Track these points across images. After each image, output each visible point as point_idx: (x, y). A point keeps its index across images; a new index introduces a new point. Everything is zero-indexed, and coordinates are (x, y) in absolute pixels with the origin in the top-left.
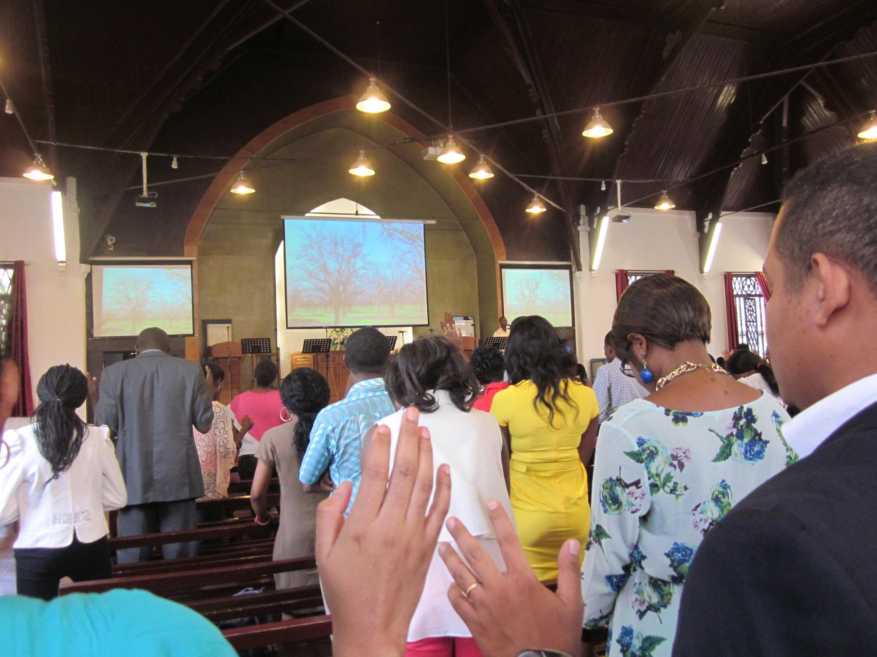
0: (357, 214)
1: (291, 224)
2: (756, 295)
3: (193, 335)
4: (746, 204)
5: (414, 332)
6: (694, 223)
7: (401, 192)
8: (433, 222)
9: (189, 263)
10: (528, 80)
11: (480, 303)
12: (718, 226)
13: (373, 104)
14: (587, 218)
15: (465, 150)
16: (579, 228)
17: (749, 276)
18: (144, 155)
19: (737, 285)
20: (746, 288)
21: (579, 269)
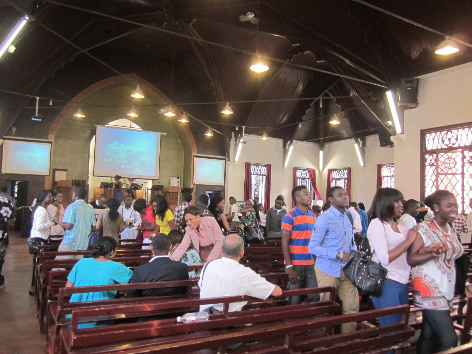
0: (130, 127)
1: (99, 128)
2: (307, 178)
3: (49, 176)
4: (307, 138)
5: (152, 182)
6: (282, 144)
7: (150, 122)
8: (165, 134)
9: (50, 142)
10: (211, 79)
12: (292, 147)
13: (138, 96)
14: (234, 138)
15: (175, 112)
16: (231, 142)
17: (304, 170)
18: (38, 98)
19: (299, 174)
20: (303, 175)
21: (229, 161)
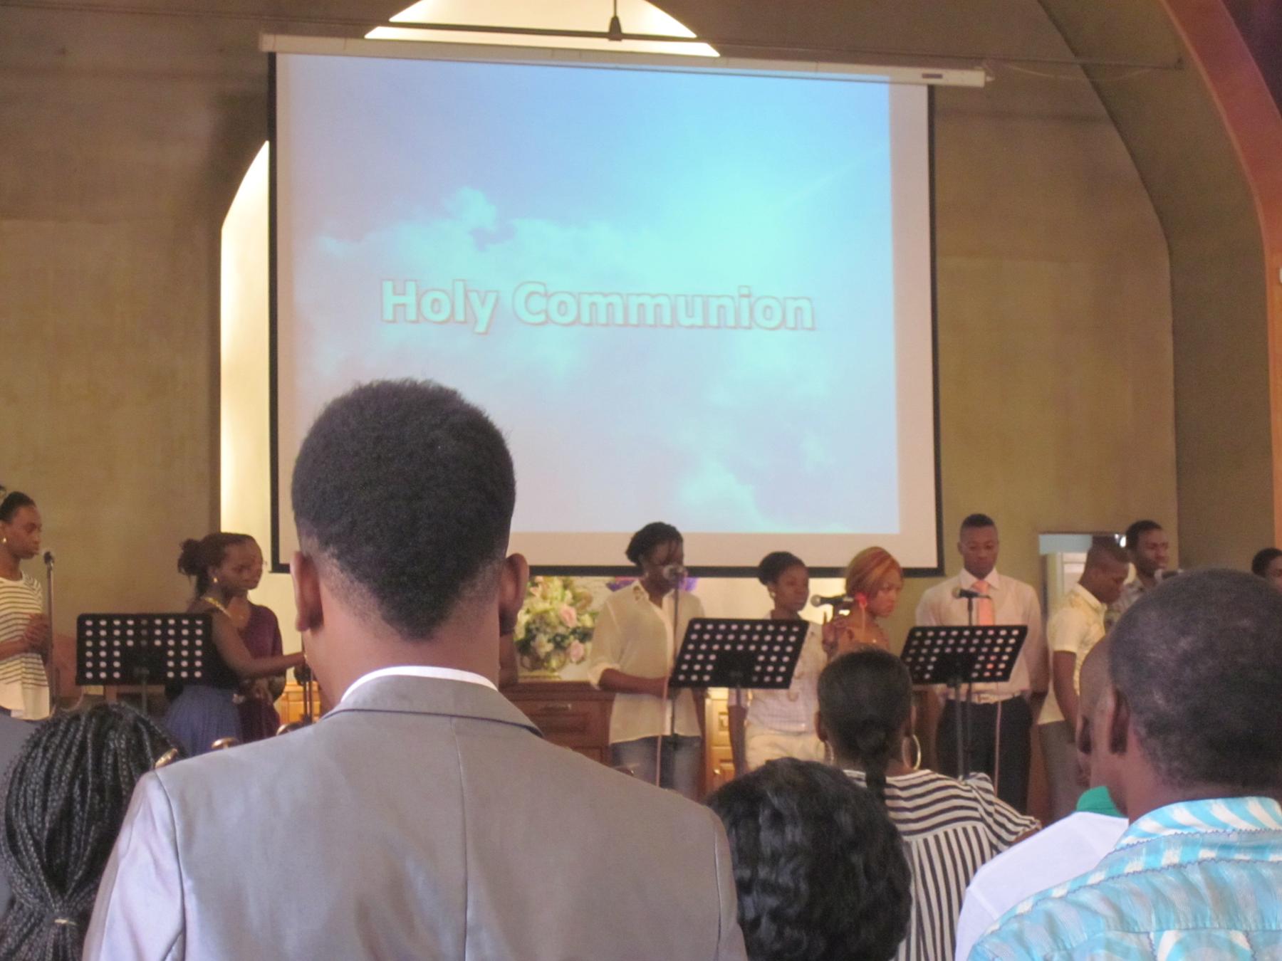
0: (615, 31)
1: (310, 73)
8: (975, 78)
11: (1183, 469)
